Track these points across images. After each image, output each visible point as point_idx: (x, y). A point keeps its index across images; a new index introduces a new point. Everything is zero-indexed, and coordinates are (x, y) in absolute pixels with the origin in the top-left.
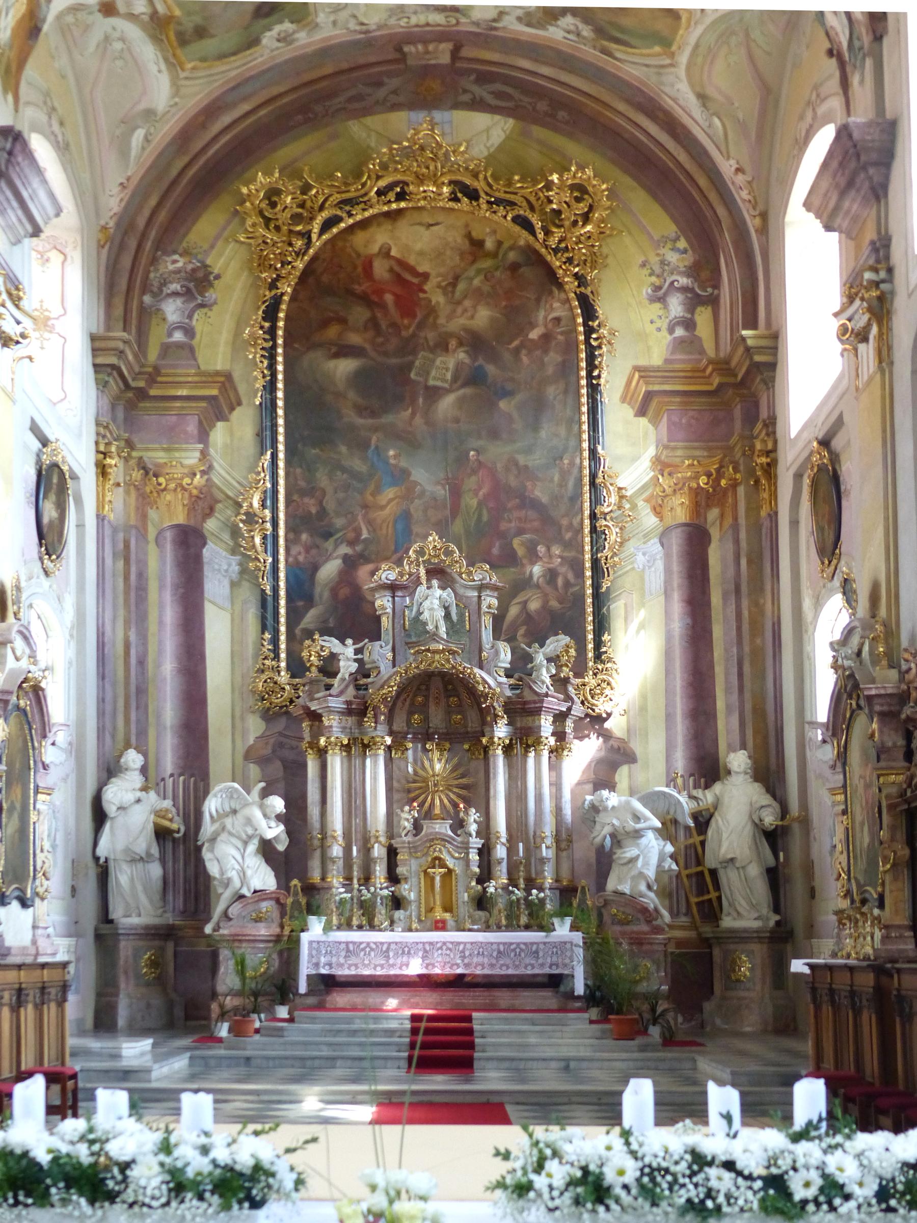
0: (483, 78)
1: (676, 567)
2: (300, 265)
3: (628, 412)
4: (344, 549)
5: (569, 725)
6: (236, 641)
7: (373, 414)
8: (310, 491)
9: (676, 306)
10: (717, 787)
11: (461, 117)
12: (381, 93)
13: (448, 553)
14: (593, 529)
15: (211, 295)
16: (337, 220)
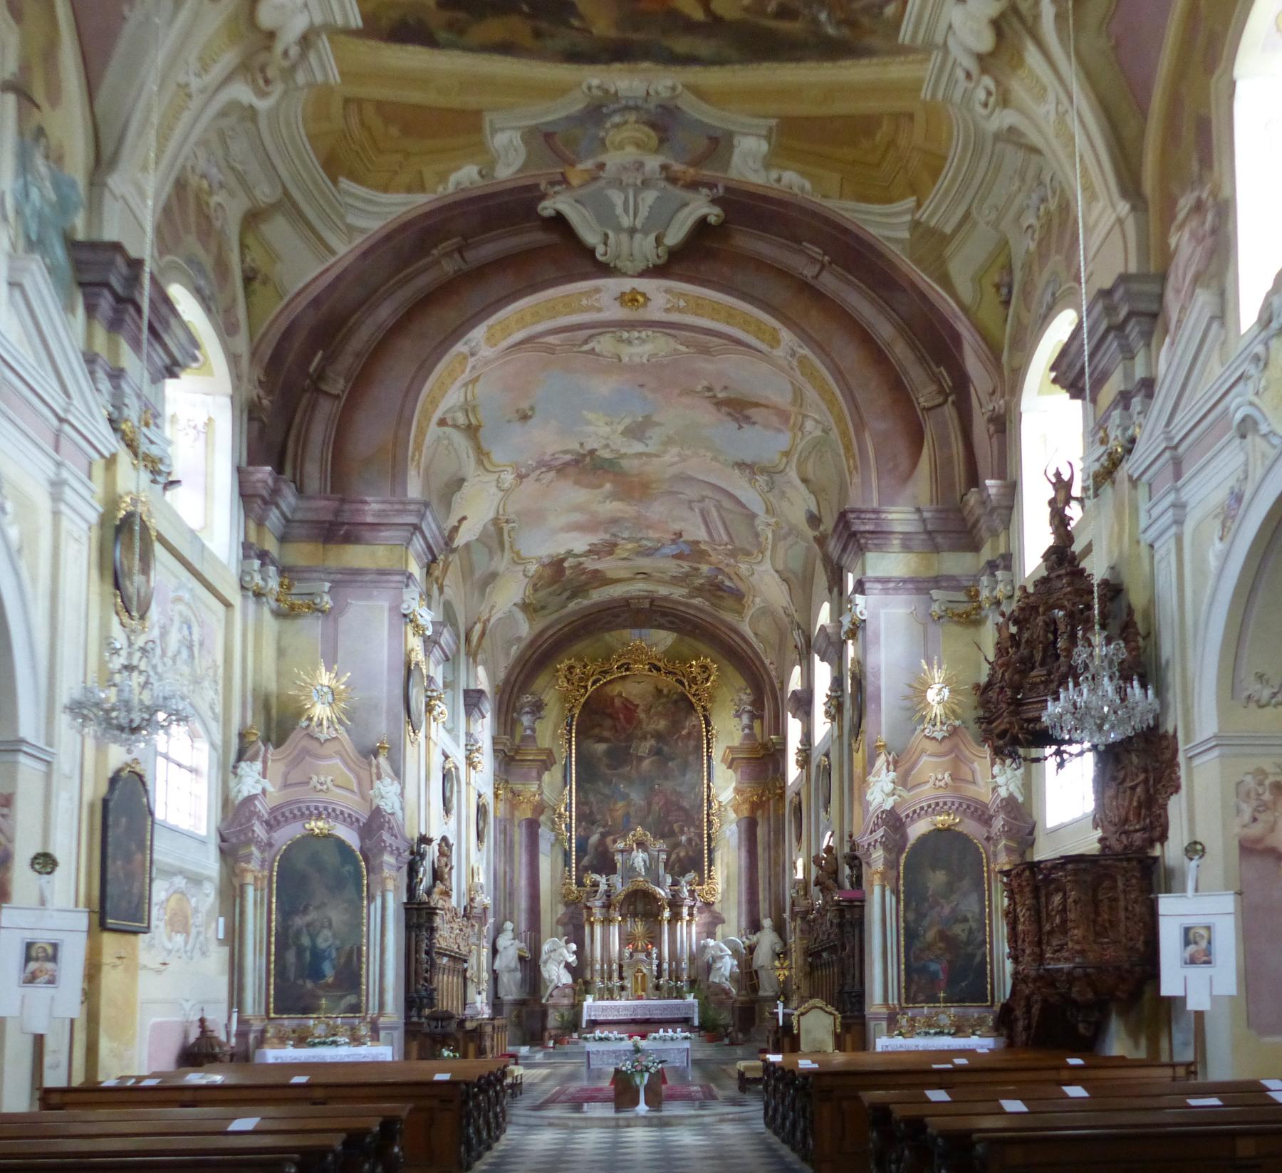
0: (664, 614)
1: (743, 836)
2: (583, 700)
3: (724, 767)
5: (695, 910)
6: (553, 869)
8: (586, 803)
9: (745, 719)
10: (758, 934)
11: (653, 631)
12: (620, 620)
15: (543, 713)
16: (598, 680)
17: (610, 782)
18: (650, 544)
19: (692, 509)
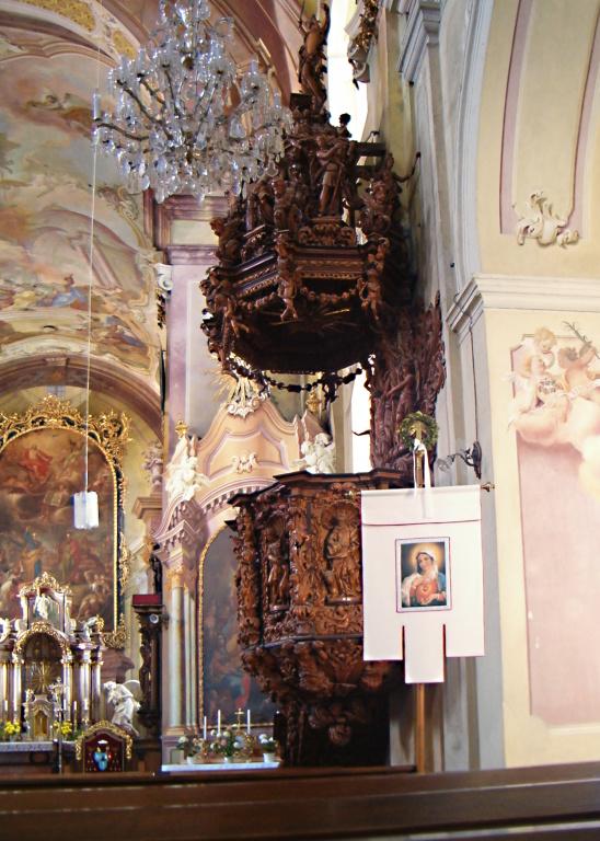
3: (135, 517)
4: (13, 577)
7: (27, 517)
11: (68, 388)
13: (51, 581)
14: (118, 569)
16: (14, 433)
17: (22, 531)
18: (46, 292)
19: (74, 248)
